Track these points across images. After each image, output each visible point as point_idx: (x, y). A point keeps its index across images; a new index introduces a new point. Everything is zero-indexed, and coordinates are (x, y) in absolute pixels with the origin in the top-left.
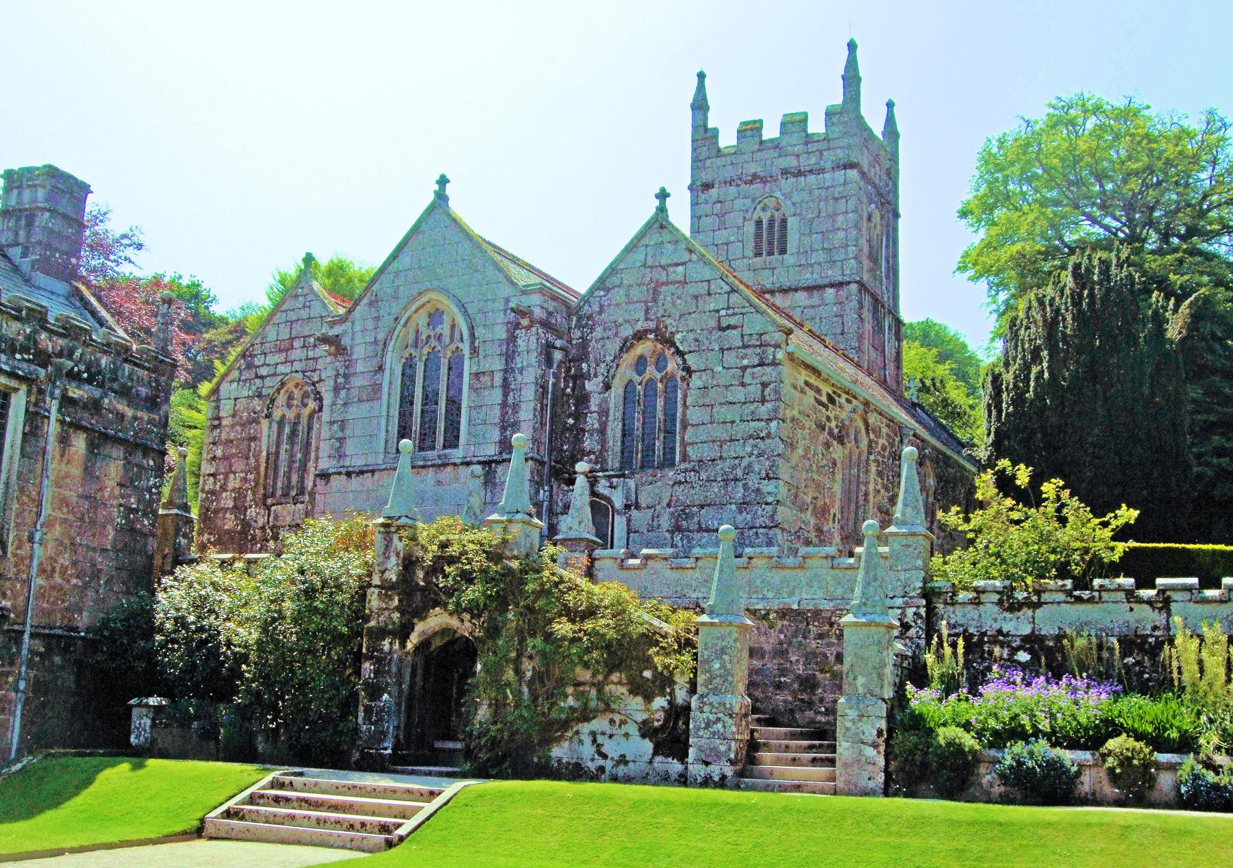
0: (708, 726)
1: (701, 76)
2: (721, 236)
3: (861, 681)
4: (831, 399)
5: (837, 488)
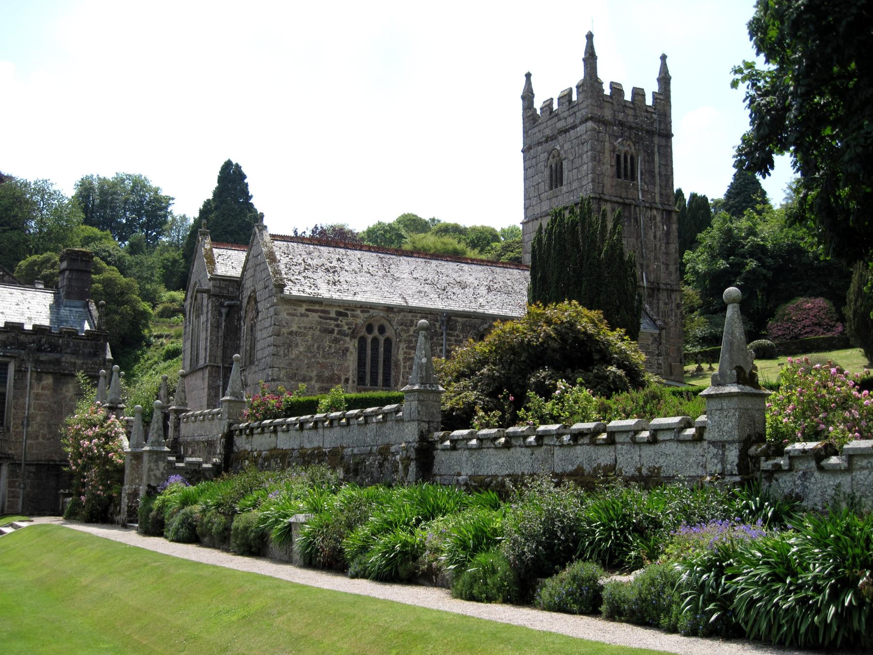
1: (528, 76)
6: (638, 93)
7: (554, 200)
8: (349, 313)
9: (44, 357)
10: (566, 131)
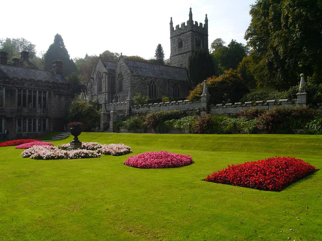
1: (171, 18)
6: (201, 24)
7: (180, 51)
8: (147, 79)
9: (56, 90)
10: (183, 33)
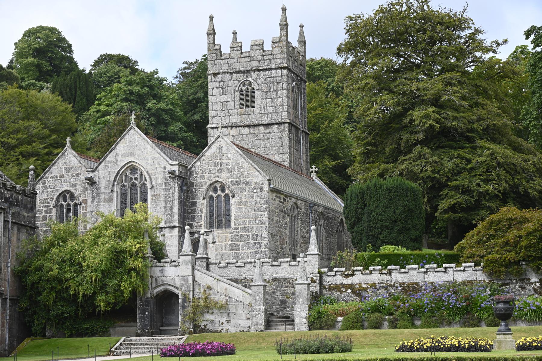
0: (256, 316)
2: (224, 98)
3: (301, 300)
4: (284, 200)
5: (287, 232)
